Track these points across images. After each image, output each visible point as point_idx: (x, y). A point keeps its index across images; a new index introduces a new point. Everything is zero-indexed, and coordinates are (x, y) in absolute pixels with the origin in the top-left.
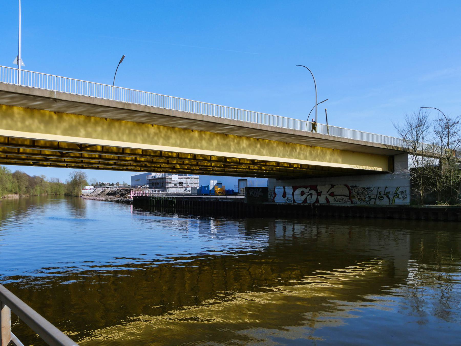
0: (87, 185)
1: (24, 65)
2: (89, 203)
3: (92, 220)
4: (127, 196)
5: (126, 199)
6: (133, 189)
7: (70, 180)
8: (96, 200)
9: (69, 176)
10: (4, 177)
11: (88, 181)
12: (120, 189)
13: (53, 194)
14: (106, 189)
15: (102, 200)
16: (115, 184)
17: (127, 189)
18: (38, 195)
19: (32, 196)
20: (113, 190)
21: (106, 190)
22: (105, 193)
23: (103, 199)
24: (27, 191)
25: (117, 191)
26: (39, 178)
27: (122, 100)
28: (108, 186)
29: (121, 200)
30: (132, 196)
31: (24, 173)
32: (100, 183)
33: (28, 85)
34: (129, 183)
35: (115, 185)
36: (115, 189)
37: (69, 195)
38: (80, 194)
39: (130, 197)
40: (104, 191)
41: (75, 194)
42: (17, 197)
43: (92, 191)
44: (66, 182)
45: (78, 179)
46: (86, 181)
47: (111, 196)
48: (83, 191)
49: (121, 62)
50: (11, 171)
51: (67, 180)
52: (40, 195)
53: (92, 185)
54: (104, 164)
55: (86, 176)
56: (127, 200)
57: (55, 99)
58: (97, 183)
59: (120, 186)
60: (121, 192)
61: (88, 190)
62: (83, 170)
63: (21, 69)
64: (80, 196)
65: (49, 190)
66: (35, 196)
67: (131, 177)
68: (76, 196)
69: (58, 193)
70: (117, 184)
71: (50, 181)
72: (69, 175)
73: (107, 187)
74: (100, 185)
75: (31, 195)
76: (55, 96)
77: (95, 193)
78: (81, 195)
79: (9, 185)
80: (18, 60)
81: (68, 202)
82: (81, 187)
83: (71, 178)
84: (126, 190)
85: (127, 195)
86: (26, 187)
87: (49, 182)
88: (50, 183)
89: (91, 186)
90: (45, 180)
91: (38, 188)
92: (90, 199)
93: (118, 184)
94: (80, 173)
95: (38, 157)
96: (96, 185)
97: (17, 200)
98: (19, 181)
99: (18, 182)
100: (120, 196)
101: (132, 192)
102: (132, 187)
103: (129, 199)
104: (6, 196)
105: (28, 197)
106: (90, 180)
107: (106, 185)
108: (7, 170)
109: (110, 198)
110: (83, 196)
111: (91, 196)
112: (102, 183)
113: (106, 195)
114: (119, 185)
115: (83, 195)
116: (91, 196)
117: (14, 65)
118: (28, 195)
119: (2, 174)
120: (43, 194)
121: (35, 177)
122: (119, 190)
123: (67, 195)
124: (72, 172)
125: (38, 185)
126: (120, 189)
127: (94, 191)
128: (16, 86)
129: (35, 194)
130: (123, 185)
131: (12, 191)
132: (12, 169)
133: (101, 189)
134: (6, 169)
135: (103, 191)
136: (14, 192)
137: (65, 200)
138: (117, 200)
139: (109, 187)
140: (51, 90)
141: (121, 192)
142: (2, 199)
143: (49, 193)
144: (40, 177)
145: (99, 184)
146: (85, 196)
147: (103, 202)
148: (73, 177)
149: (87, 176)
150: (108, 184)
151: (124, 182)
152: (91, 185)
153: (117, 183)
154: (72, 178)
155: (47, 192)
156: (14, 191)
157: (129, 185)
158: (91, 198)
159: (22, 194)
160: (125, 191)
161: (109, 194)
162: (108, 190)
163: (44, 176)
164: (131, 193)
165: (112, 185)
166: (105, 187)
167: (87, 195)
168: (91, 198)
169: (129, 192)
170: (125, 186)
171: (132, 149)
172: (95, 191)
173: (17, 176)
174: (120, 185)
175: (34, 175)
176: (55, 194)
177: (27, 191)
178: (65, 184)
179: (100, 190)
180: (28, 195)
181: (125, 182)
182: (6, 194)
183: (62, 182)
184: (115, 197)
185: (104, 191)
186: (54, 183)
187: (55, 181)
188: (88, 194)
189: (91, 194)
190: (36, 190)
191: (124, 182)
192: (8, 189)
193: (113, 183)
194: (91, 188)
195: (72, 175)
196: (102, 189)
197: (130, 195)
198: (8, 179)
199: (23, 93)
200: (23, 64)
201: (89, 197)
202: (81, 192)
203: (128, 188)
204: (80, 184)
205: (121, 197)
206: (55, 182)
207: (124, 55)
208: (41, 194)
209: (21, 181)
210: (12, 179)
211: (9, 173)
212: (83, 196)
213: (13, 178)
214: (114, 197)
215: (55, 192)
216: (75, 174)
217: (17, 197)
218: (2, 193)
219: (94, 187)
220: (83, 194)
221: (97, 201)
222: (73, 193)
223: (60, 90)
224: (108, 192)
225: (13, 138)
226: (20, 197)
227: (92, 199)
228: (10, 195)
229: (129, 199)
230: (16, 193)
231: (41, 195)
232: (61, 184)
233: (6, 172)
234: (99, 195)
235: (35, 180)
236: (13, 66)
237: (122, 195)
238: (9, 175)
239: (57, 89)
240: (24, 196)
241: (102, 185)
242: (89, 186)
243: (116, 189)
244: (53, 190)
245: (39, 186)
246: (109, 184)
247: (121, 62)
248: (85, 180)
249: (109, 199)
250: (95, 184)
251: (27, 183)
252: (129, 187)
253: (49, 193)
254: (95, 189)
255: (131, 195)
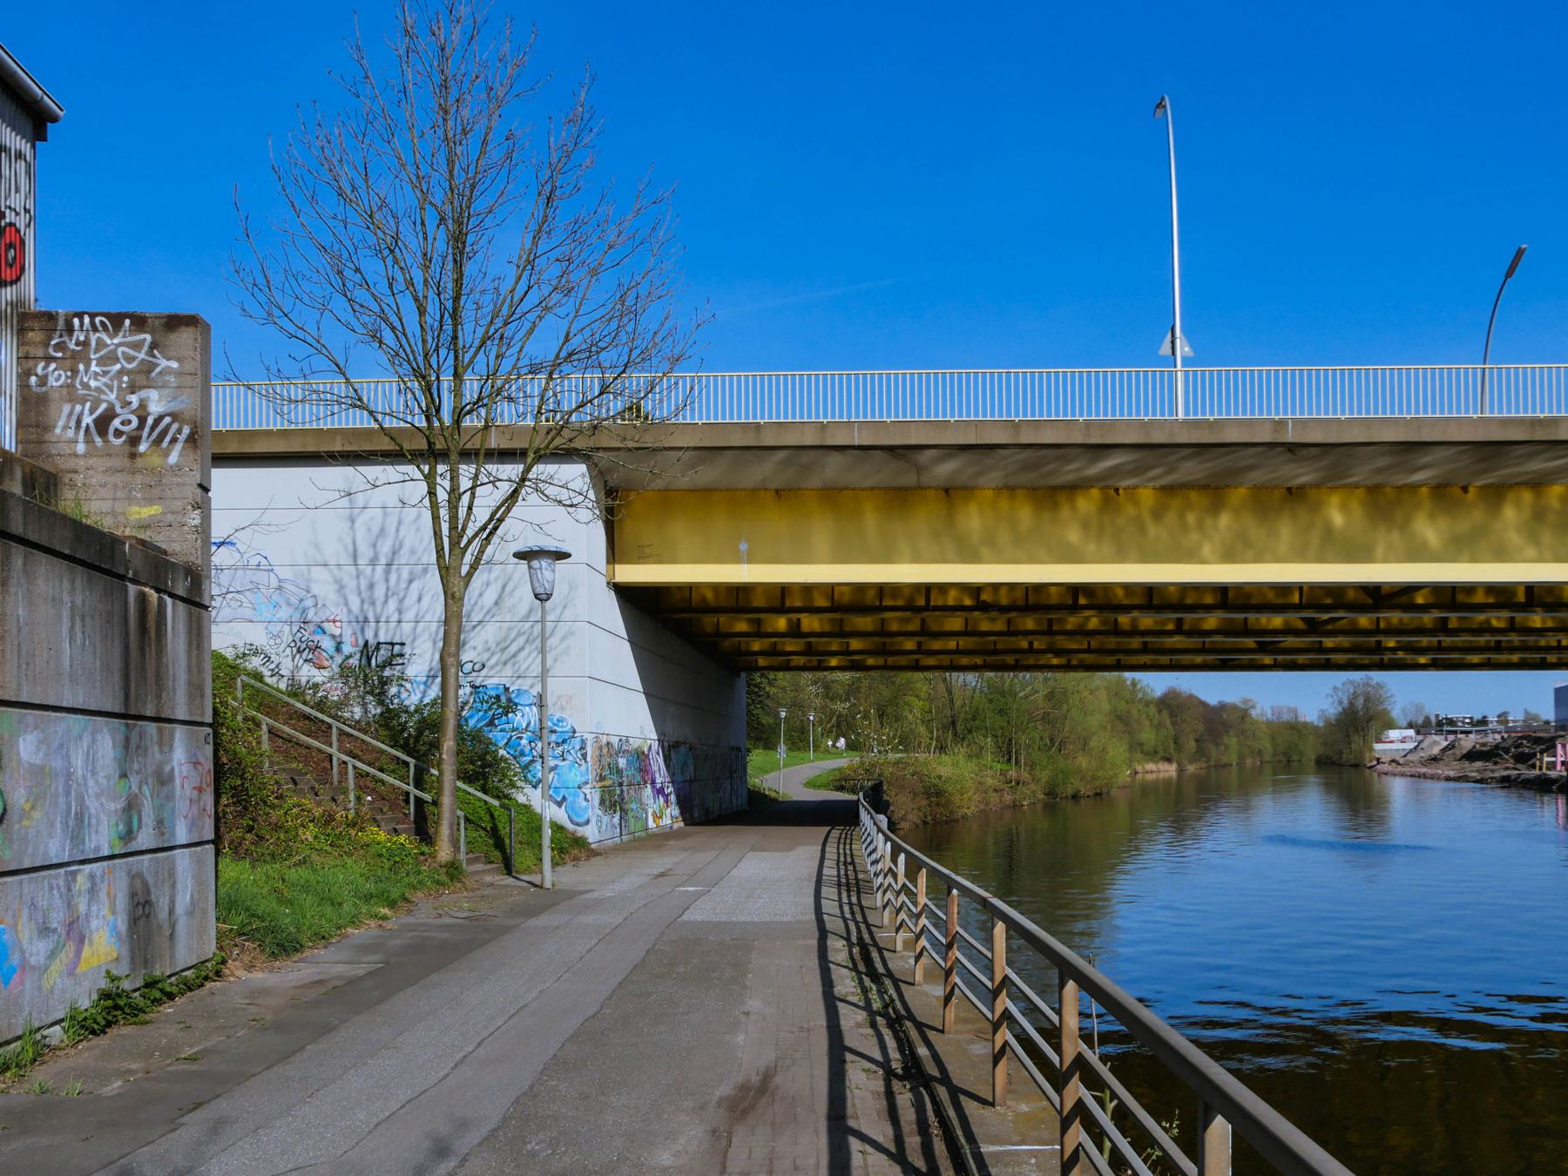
0: (1391, 725)
1: (1192, 354)
2: (1398, 789)
3: (1415, 848)
4: (1542, 763)
5: (1537, 772)
6: (1562, 736)
7: (1332, 710)
8: (1424, 776)
9: (1331, 699)
10: (1135, 712)
11: (1396, 713)
12: (1513, 735)
13: (1280, 761)
14: (1460, 739)
15: (1448, 779)
16: (1492, 718)
17: (1539, 735)
18: (1231, 765)
19: (1215, 766)
20: (1485, 740)
21: (1462, 742)
22: (1459, 753)
23: (1452, 774)
24: (1201, 753)
25: (1502, 745)
26: (1234, 708)
27: (1526, 411)
28: (1468, 728)
29: (1520, 775)
30: (1563, 763)
31: (1191, 697)
32: (1437, 716)
33: (1271, 414)
34: (1547, 711)
35: (1492, 722)
36: (1493, 739)
37: (1333, 763)
38: (1368, 760)
39: (1552, 766)
40: (1454, 747)
41: (1351, 756)
42: (1169, 770)
43: (1411, 745)
44: (1319, 717)
45: (1360, 707)
46: (1388, 712)
47: (1479, 764)
48: (1378, 747)
49: (1510, 273)
50: (1152, 690)
51: (1322, 711)
52: (1237, 764)
53: (1410, 726)
54: (1523, 648)
55: (1388, 695)
56: (1540, 776)
57: (1290, 443)
58: (1427, 719)
59: (1510, 725)
60: (1517, 747)
61: (1397, 741)
62: (1377, 676)
63: (1183, 366)
64: (1369, 765)
65: (1267, 745)
66: (1224, 766)
67: (1558, 691)
68: (1356, 766)
69: (1295, 758)
70: (1502, 718)
71: (1269, 716)
72: (1332, 696)
73: (1462, 732)
74: (1440, 724)
75: (1212, 763)
76: (1290, 436)
77: (1422, 754)
78: (1371, 761)
79: (1148, 736)
80: (1173, 343)
81: (1328, 787)
82: (1372, 733)
83: (1336, 702)
84: (1538, 741)
85: (1541, 760)
86: (1197, 741)
87: (1267, 720)
88: (1269, 723)
89: (1406, 728)
90: (1253, 713)
91: (1232, 741)
92: (1403, 775)
93: (1503, 718)
94: (1367, 684)
95: (1177, 641)
96: (1423, 727)
97: (1170, 778)
98: (1176, 722)
99: (1174, 724)
100: (1512, 761)
101: (1559, 747)
102: (1558, 728)
103: (1549, 773)
104: (1139, 768)
105: (1204, 771)
106: (1404, 710)
107: (1460, 724)
108: (1141, 688)
109: (1478, 771)
110: (1378, 767)
111: (1406, 764)
112: (1446, 719)
113: (1460, 760)
114: (1508, 722)
115: (1378, 759)
116: (1406, 764)
117: (1165, 357)
118: (1204, 765)
119: (1127, 703)
120: (1248, 762)
121: (1223, 707)
122: (1510, 742)
123: (1326, 763)
124: (1339, 685)
125: (1232, 732)
126: (1513, 735)
127: (1416, 748)
128: (1171, 421)
129: (1225, 760)
130: (1524, 721)
131: (1156, 752)
132: (1156, 683)
133: (1443, 737)
134: (1139, 686)
135: (1451, 746)
136: (1163, 755)
137: (1317, 780)
138: (1504, 777)
139: (1470, 732)
140: (1277, 418)
141: (1517, 747)
142: (1129, 779)
143: (1267, 758)
144: (1239, 704)
145: (1433, 720)
146: (1387, 765)
147: (1452, 785)
148: (1346, 702)
149: (1392, 696)
150: (1467, 721)
151: (1527, 712)
152: (1405, 723)
153: (1499, 716)
154: (1340, 702)
155: (1260, 752)
156: (1162, 754)
157: (1547, 723)
158: (1406, 769)
159: (1186, 762)
160: (1534, 743)
161: (1471, 756)
162: (1468, 742)
163: (1251, 700)
164: (1556, 752)
165: (1483, 722)
166: (1455, 732)
167: (1393, 761)
168: (1406, 769)
169: (1549, 745)
170: (1530, 726)
171: (1491, 588)
172: (1423, 745)
173: (1172, 704)
174: (1514, 721)
175: (1220, 699)
176: (1285, 760)
177: (1201, 753)
178: (1318, 726)
179: (1436, 743)
180: (1204, 765)
181: (1533, 710)
182: (1139, 763)
183: (1308, 719)
184: (1494, 767)
185: (1454, 747)
186: (1283, 722)
187: (1286, 717)
188: (1397, 759)
189: (1405, 756)
190: (1227, 747)
191: (1527, 712)
192: (1145, 747)
193: (1485, 717)
194: (1405, 738)
195: (1340, 693)
196: (1446, 740)
197: (1553, 759)
198: (1144, 715)
199: (1193, 440)
200: (1187, 349)
201: (1400, 768)
202: (1371, 749)
203: (1545, 731)
204: (1368, 722)
205: (1519, 766)
206: (1285, 719)
207: (1524, 246)
208: (1242, 758)
209: (1184, 721)
210: (1157, 716)
211: (1149, 698)
212: (1378, 763)
213: (1160, 711)
214: (1490, 766)
215: (1284, 754)
216: (1352, 691)
217: (1169, 770)
218: (1130, 761)
219: (1418, 733)
220: (1377, 756)
221: (1429, 781)
222: (1345, 756)
223: (1271, 414)
224: (1468, 749)
225: (1239, 588)
226: (1181, 770)
227: (1412, 776)
228: (1150, 766)
229: (1549, 773)
230: (1169, 760)
231: (1241, 765)
232: (1306, 724)
233: (1140, 696)
234: (1434, 759)
235: (1224, 715)
236: (1162, 361)
237: (1522, 758)
238: (1147, 704)
239: (1293, 413)
240: (1191, 768)
241: (1444, 725)
242: (1397, 731)
243: (1498, 737)
244: (1277, 745)
245: (1237, 736)
246: (1471, 718)
247: (1510, 273)
248: (1383, 710)
249: (1474, 774)
250: (1420, 721)
251: (1201, 727)
252: (1547, 727)
253: (1267, 758)
254: (1420, 738)
255: (1559, 755)
